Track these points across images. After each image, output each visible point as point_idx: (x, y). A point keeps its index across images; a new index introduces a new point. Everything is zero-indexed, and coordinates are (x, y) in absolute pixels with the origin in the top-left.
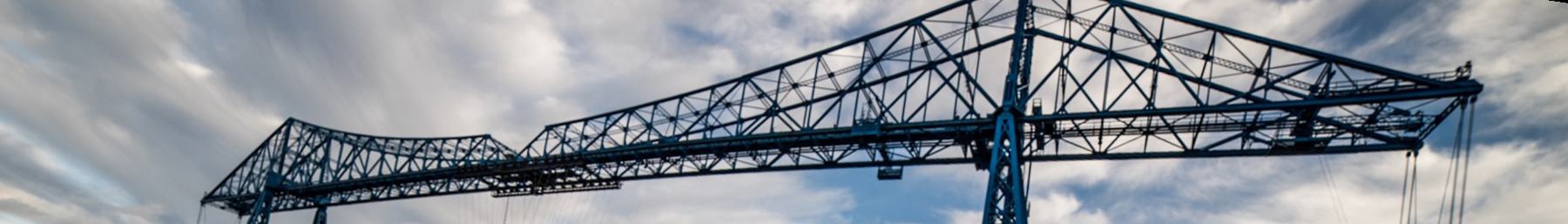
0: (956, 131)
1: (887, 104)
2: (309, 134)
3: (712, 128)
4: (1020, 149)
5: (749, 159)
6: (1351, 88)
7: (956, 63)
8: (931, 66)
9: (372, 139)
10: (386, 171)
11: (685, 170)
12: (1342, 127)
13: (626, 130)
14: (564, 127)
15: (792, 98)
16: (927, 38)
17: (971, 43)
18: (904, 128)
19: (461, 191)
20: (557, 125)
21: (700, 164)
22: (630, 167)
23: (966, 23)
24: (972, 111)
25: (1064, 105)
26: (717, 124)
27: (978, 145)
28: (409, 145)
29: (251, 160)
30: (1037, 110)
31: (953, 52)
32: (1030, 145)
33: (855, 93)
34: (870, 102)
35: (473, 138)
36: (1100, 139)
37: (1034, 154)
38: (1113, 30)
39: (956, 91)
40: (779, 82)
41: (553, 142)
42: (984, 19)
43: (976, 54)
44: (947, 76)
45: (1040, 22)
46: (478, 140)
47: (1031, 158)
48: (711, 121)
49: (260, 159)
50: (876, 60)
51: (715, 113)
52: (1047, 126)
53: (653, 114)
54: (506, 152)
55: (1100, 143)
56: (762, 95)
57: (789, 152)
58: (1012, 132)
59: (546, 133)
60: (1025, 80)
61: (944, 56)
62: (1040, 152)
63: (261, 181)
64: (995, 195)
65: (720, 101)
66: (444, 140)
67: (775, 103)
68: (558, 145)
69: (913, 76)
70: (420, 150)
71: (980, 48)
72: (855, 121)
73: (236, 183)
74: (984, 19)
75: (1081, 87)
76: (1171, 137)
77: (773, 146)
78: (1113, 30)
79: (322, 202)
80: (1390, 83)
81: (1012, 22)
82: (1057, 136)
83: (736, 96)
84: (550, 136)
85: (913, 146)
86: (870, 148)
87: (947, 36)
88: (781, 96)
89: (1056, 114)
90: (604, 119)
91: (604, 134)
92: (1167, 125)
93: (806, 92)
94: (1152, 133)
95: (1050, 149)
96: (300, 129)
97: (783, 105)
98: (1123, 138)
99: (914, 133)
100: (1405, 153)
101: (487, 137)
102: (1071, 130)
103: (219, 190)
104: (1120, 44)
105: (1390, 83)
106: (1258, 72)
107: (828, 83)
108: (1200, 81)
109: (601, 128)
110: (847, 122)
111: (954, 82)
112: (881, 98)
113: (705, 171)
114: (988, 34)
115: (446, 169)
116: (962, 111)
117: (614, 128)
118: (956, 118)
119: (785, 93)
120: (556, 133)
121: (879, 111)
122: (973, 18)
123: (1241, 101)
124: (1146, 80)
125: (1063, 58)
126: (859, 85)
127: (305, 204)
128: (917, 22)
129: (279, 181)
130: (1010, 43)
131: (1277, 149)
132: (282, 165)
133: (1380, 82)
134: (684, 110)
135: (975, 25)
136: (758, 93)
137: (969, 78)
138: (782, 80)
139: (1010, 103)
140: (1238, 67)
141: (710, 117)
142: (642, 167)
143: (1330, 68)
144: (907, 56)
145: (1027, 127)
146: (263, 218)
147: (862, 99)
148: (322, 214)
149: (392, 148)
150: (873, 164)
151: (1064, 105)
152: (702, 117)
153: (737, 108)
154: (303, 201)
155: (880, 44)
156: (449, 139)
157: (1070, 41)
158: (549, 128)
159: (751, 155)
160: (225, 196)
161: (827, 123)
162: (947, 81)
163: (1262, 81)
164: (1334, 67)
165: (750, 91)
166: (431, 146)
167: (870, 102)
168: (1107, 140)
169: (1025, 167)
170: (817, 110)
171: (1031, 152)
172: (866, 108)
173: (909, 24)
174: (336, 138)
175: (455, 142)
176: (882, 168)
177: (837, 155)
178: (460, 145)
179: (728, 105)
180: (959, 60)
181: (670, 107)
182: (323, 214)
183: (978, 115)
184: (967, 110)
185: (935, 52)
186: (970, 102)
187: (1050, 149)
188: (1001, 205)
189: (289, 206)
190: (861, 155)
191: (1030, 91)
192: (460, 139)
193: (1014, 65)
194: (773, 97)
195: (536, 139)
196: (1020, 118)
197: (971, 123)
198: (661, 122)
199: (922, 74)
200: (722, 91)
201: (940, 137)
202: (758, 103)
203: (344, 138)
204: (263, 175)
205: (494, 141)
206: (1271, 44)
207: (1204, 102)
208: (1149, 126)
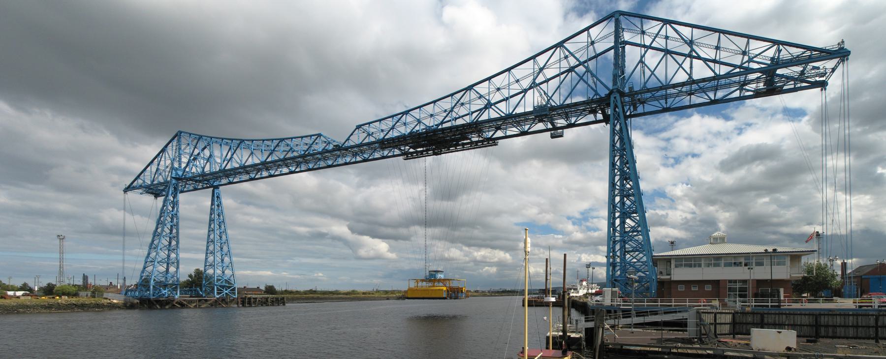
3: (456, 119)
6: (790, 58)
12: (789, 78)
13: (405, 124)
16: (567, 53)
23: (588, 42)
26: (457, 116)
30: (631, 89)
31: (582, 60)
32: (629, 109)
34: (541, 95)
36: (666, 101)
37: (632, 113)
40: (489, 88)
42: (596, 39)
47: (631, 116)
50: (541, 70)
55: (666, 103)
56: (481, 97)
61: (578, 63)
62: (635, 112)
65: (458, 102)
72: (534, 107)
74: (596, 39)
78: (667, 38)
80: (808, 53)
82: (643, 102)
83: (465, 99)
86: (545, 122)
88: (491, 96)
91: (393, 128)
95: (640, 109)
97: (493, 102)
102: (650, 97)
105: (808, 53)
106: (744, 53)
108: (714, 61)
111: (585, 78)
112: (546, 92)
117: (398, 124)
119: (493, 94)
121: (546, 99)
122: (591, 39)
123: (738, 70)
126: (534, 85)
135: (593, 43)
136: (478, 96)
138: (490, 87)
139: (616, 87)
140: (733, 51)
143: (779, 48)
147: (537, 94)
152: (449, 113)
157: (644, 46)
163: (746, 58)
164: (781, 47)
167: (541, 95)
168: (670, 101)
171: (631, 112)
176: (552, 132)
180: (586, 64)
187: (640, 109)
190: (540, 126)
194: (487, 98)
198: (425, 118)
199: (568, 74)
202: (479, 101)
208: (691, 90)
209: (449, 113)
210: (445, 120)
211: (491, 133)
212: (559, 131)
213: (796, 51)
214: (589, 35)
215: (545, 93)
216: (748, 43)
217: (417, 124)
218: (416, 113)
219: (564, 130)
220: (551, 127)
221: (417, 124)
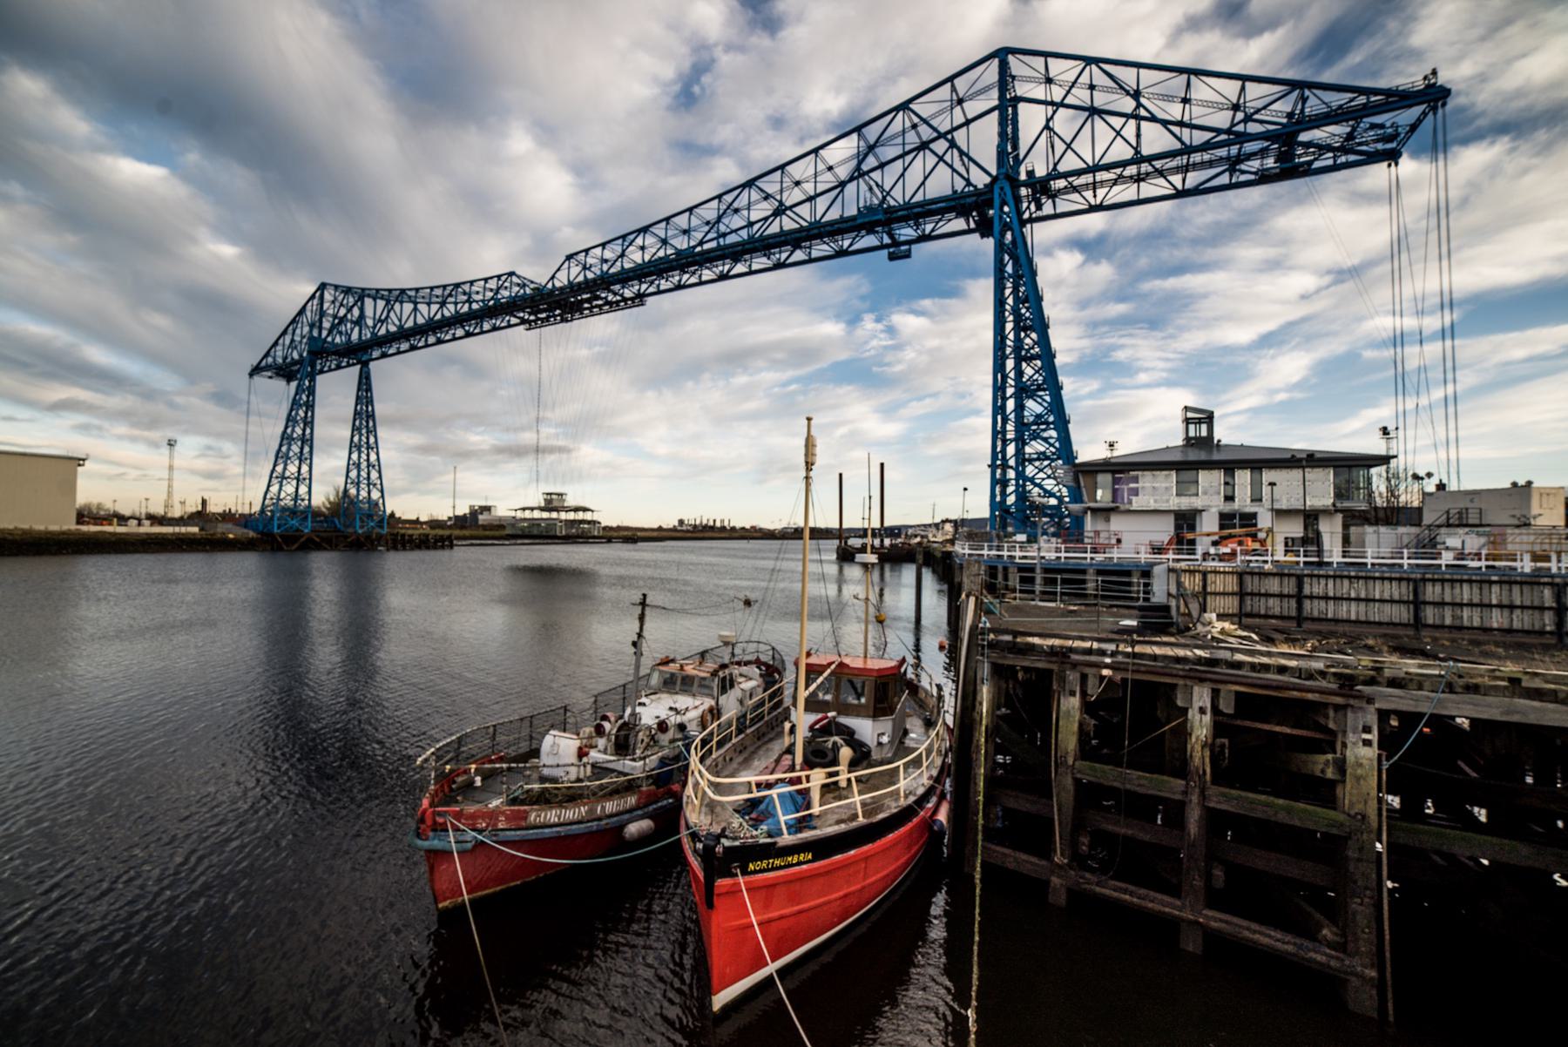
0: (956, 204)
1: (887, 188)
3: (724, 235)
4: (1019, 213)
5: (764, 260)
7: (947, 140)
8: (924, 146)
9: (403, 291)
10: (420, 321)
11: (704, 278)
13: (643, 248)
15: (795, 196)
16: (916, 120)
17: (959, 118)
18: (907, 209)
19: (495, 329)
20: (577, 254)
21: (717, 270)
22: (652, 283)
24: (969, 183)
25: (1056, 165)
27: (979, 215)
28: (438, 292)
30: (1030, 173)
31: (943, 129)
32: (1028, 208)
33: (855, 182)
34: (871, 189)
35: (499, 277)
38: (1092, 87)
39: (951, 166)
41: (575, 270)
43: (965, 129)
44: (940, 154)
45: (1021, 89)
46: (503, 278)
47: (1032, 220)
48: (723, 228)
50: (871, 148)
51: (725, 220)
52: (1042, 188)
54: (532, 286)
56: (767, 197)
57: (800, 248)
58: (1009, 198)
60: (1015, 147)
61: (935, 135)
62: (1039, 213)
64: (1002, 260)
65: (728, 208)
66: (472, 283)
67: (781, 203)
69: (908, 158)
70: (450, 295)
71: (968, 122)
73: (279, 353)
75: (1069, 146)
76: (1161, 181)
77: (785, 243)
78: (1092, 87)
80: (1362, 100)
81: (995, 93)
82: (1053, 196)
83: (743, 201)
85: (918, 225)
87: (934, 116)
88: (785, 195)
89: (1048, 174)
90: (620, 241)
91: (622, 255)
92: (1156, 170)
93: (809, 188)
94: (1143, 180)
95: (1048, 209)
97: (788, 204)
98: (1116, 189)
99: (917, 212)
100: (1386, 164)
101: (511, 274)
104: (1100, 100)
105: (1362, 100)
106: (1236, 107)
107: (828, 176)
108: (1181, 124)
109: (619, 249)
110: (852, 211)
111: (948, 158)
113: (723, 277)
114: (973, 108)
115: (477, 311)
116: (960, 184)
117: (631, 248)
118: (955, 192)
121: (880, 196)
123: (1223, 137)
124: (1130, 130)
125: (1048, 121)
126: (858, 174)
128: (904, 106)
129: (320, 344)
130: (996, 113)
131: (1264, 178)
133: (1352, 100)
134: (695, 222)
135: (960, 102)
137: (961, 153)
139: (1003, 171)
142: (663, 282)
144: (900, 140)
145: (1024, 191)
147: (863, 187)
150: (882, 247)
151: (1056, 165)
153: (745, 213)
155: (872, 132)
157: (1052, 103)
158: (569, 257)
161: (834, 215)
162: (941, 159)
163: (1240, 116)
164: (1307, 93)
165: (755, 195)
167: (871, 189)
168: (1101, 192)
169: (1027, 229)
170: (822, 204)
172: (868, 195)
173: (897, 109)
174: (369, 296)
175: (482, 283)
177: (846, 243)
179: (736, 211)
180: (949, 137)
181: (682, 221)
183: (975, 187)
184: (964, 183)
185: (926, 133)
186: (966, 175)
187: (1048, 209)
188: (1009, 269)
190: (869, 240)
191: (1021, 157)
192: (486, 280)
193: (1002, 134)
194: (778, 197)
196: (1015, 184)
197: (970, 195)
198: (675, 236)
200: (728, 198)
201: (942, 212)
202: (765, 205)
203: (376, 294)
205: (519, 277)
206: (1244, 78)
207: (1188, 143)
208: (1139, 174)
213: (1337, 99)
214: (954, 89)
215: (877, 185)
216: (1243, 88)
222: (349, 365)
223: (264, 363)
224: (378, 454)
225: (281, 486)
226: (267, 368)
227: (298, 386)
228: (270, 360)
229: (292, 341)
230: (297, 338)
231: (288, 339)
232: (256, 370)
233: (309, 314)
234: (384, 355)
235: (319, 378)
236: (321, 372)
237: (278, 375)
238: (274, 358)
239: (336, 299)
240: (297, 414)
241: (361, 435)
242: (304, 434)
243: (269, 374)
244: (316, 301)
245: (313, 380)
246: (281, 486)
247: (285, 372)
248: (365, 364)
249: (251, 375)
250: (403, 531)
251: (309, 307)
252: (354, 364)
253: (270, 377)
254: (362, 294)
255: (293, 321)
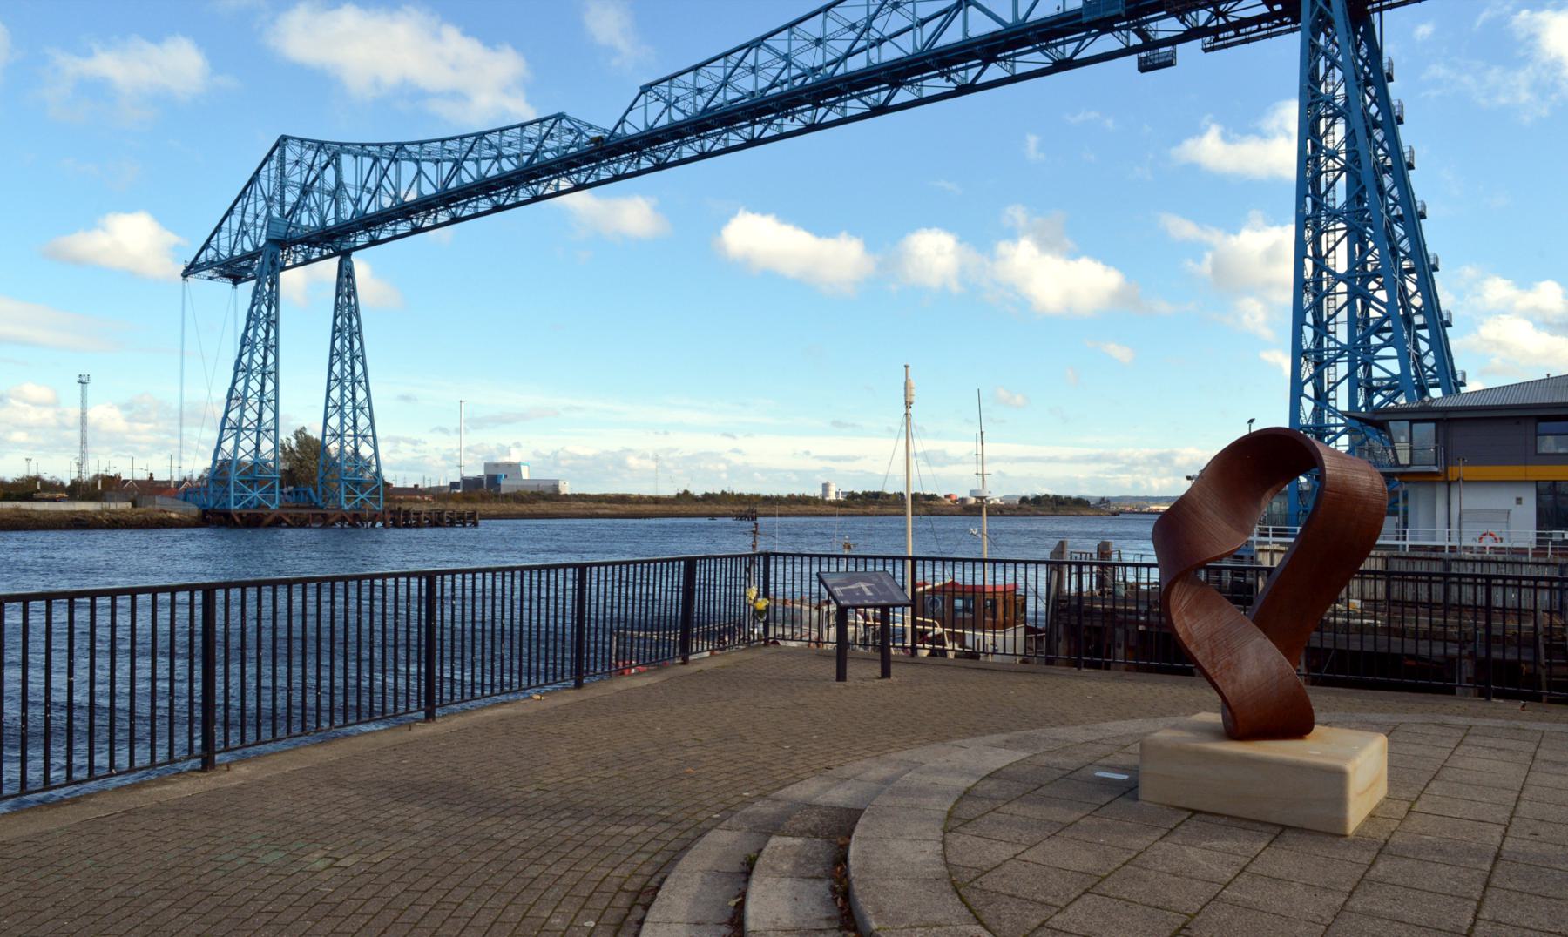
2: (311, 153)
5: (941, 81)
10: (428, 190)
13: (754, 69)
14: (666, 83)
19: (536, 198)
20: (657, 83)
22: (770, 122)
29: (240, 203)
41: (656, 108)
49: (252, 200)
53: (790, 40)
57: (996, 60)
59: (643, 96)
63: (258, 231)
68: (663, 112)
70: (471, 150)
79: (343, 248)
84: (650, 100)
86: (1119, 29)
91: (725, 83)
96: (298, 149)
101: (560, 117)
103: (203, 254)
115: (512, 174)
117: (739, 70)
120: (657, 93)
127: (321, 253)
132: (282, 204)
134: (832, 27)
141: (872, 31)
142: (787, 121)
146: (271, 285)
148: (346, 263)
149: (429, 153)
150: (1128, 51)
154: (317, 249)
156: (507, 128)
158: (646, 89)
159: (941, 75)
160: (212, 262)
166: (485, 141)
174: (349, 152)
176: (1143, 55)
177: (1070, 49)
178: (525, 134)
182: (348, 263)
189: (300, 260)
190: (1108, 42)
195: (630, 109)
198: (802, 50)
203: (360, 150)
204: (260, 222)
209: (864, 31)
210: (854, 49)
211: (972, 73)
212: (1161, 50)
217: (784, 69)
218: (780, 43)
219: (1178, 47)
220: (1139, 41)
221: (784, 69)
222: (322, 258)
223: (202, 259)
224: (368, 391)
225: (238, 441)
226: (210, 264)
227: (256, 292)
228: (211, 253)
229: (242, 223)
230: (248, 220)
231: (235, 220)
232: (192, 269)
233: (264, 182)
234: (374, 242)
235: (283, 275)
236: (284, 269)
237: (222, 275)
238: (218, 253)
239: (301, 157)
240: (255, 334)
241: (343, 363)
242: (265, 363)
243: (209, 273)
244: (274, 164)
245: (275, 282)
246: (238, 441)
247: (233, 271)
248: (345, 255)
249: (185, 274)
250: (405, 506)
251: (264, 173)
252: (329, 256)
253: (210, 278)
254: (334, 152)
255: (243, 194)
